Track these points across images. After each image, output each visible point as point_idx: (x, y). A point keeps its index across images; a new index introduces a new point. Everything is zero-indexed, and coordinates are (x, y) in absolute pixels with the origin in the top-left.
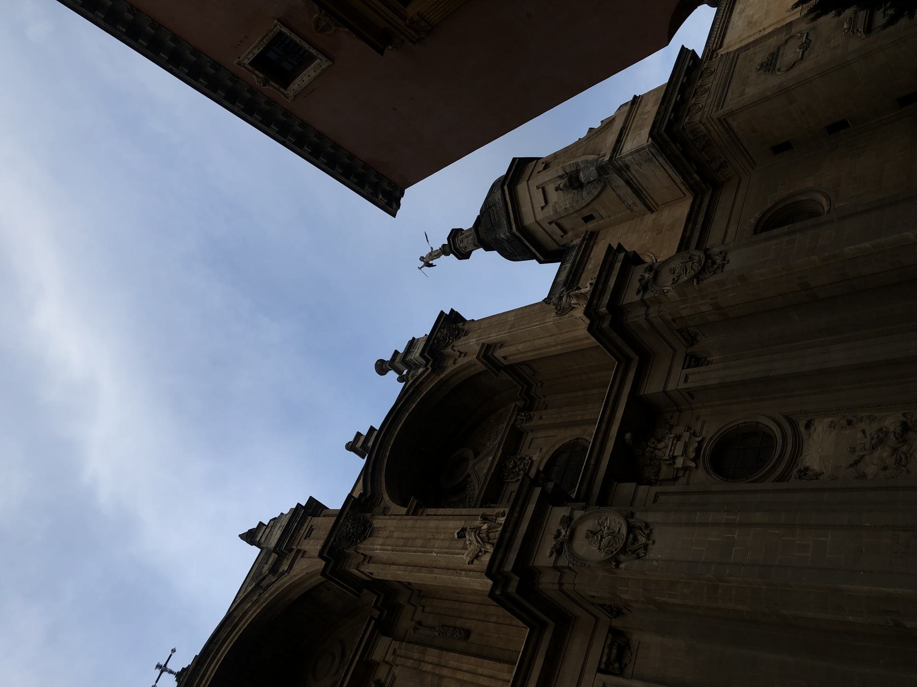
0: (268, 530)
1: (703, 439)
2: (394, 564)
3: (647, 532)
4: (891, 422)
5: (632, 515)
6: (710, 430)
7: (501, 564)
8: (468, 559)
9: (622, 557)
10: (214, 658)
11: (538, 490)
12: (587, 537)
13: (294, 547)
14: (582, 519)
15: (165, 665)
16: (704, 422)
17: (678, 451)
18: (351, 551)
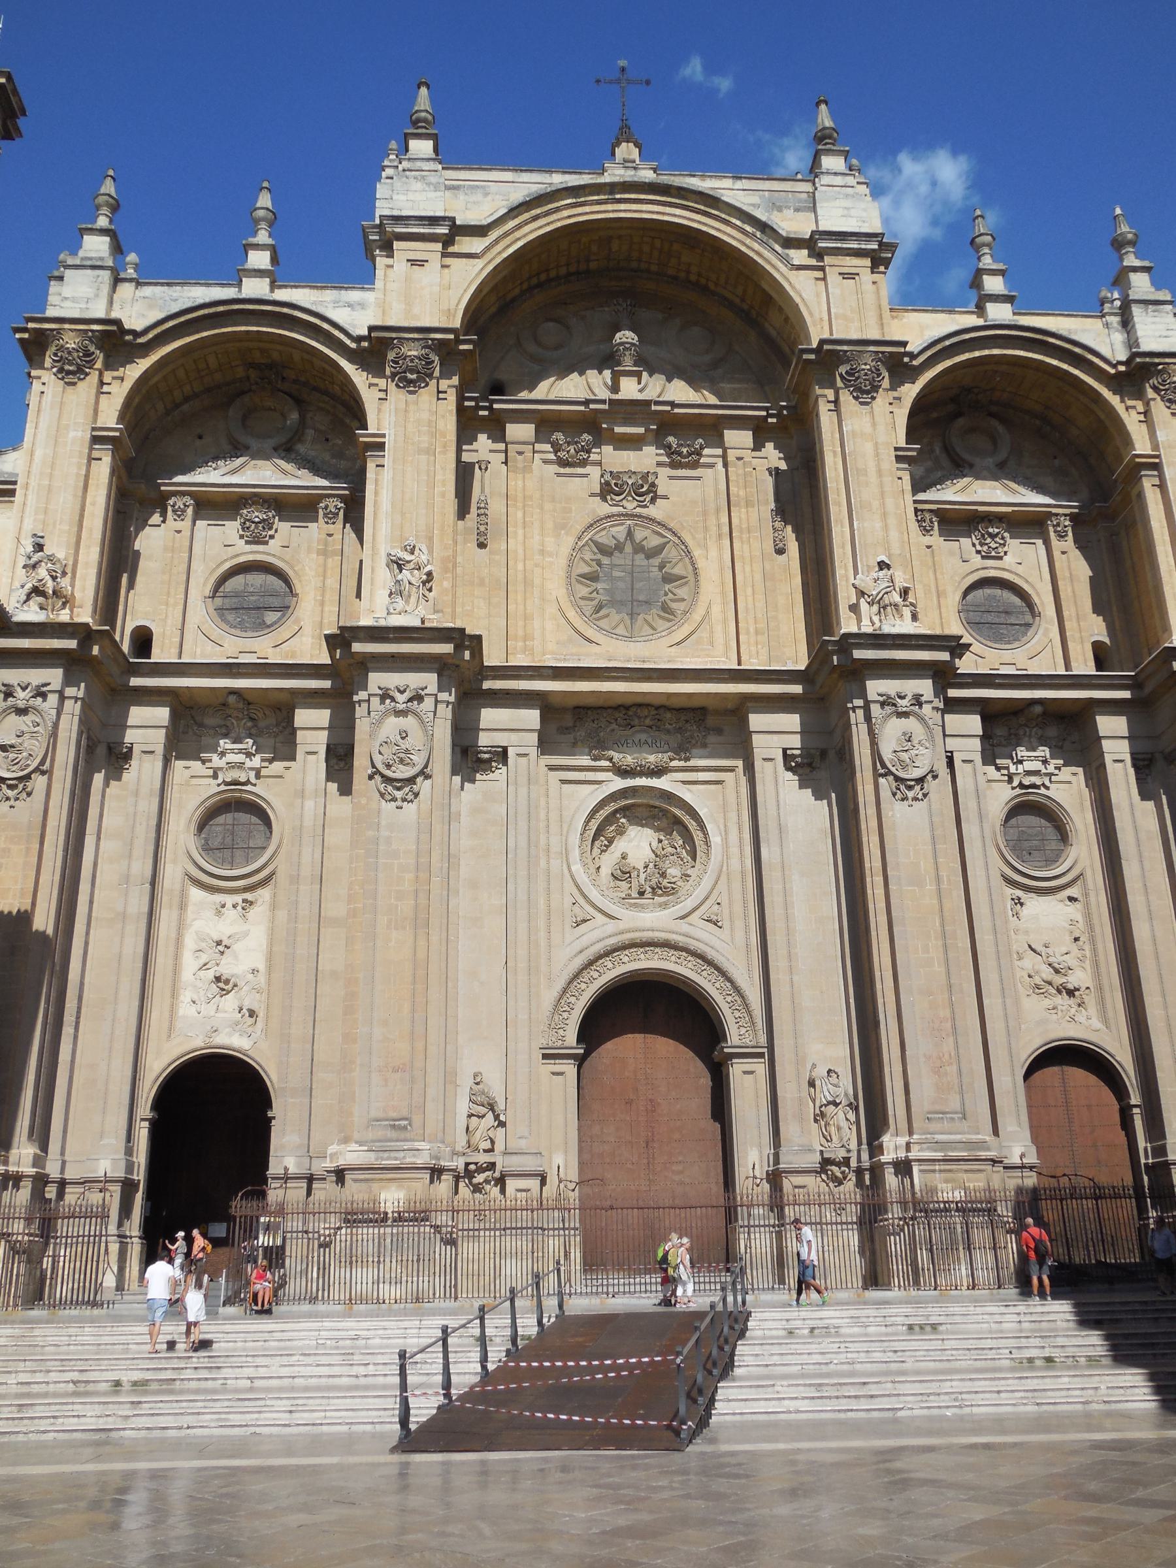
0: (839, 180)
1: (1047, 788)
3: (920, 796)
4: (1079, 978)
5: (935, 777)
6: (1058, 793)
7: (860, 646)
8: (857, 582)
9: (891, 778)
11: (945, 656)
12: (904, 734)
14: (921, 719)
15: (629, 82)
16: (1070, 782)
17: (1028, 766)
18: (839, 383)
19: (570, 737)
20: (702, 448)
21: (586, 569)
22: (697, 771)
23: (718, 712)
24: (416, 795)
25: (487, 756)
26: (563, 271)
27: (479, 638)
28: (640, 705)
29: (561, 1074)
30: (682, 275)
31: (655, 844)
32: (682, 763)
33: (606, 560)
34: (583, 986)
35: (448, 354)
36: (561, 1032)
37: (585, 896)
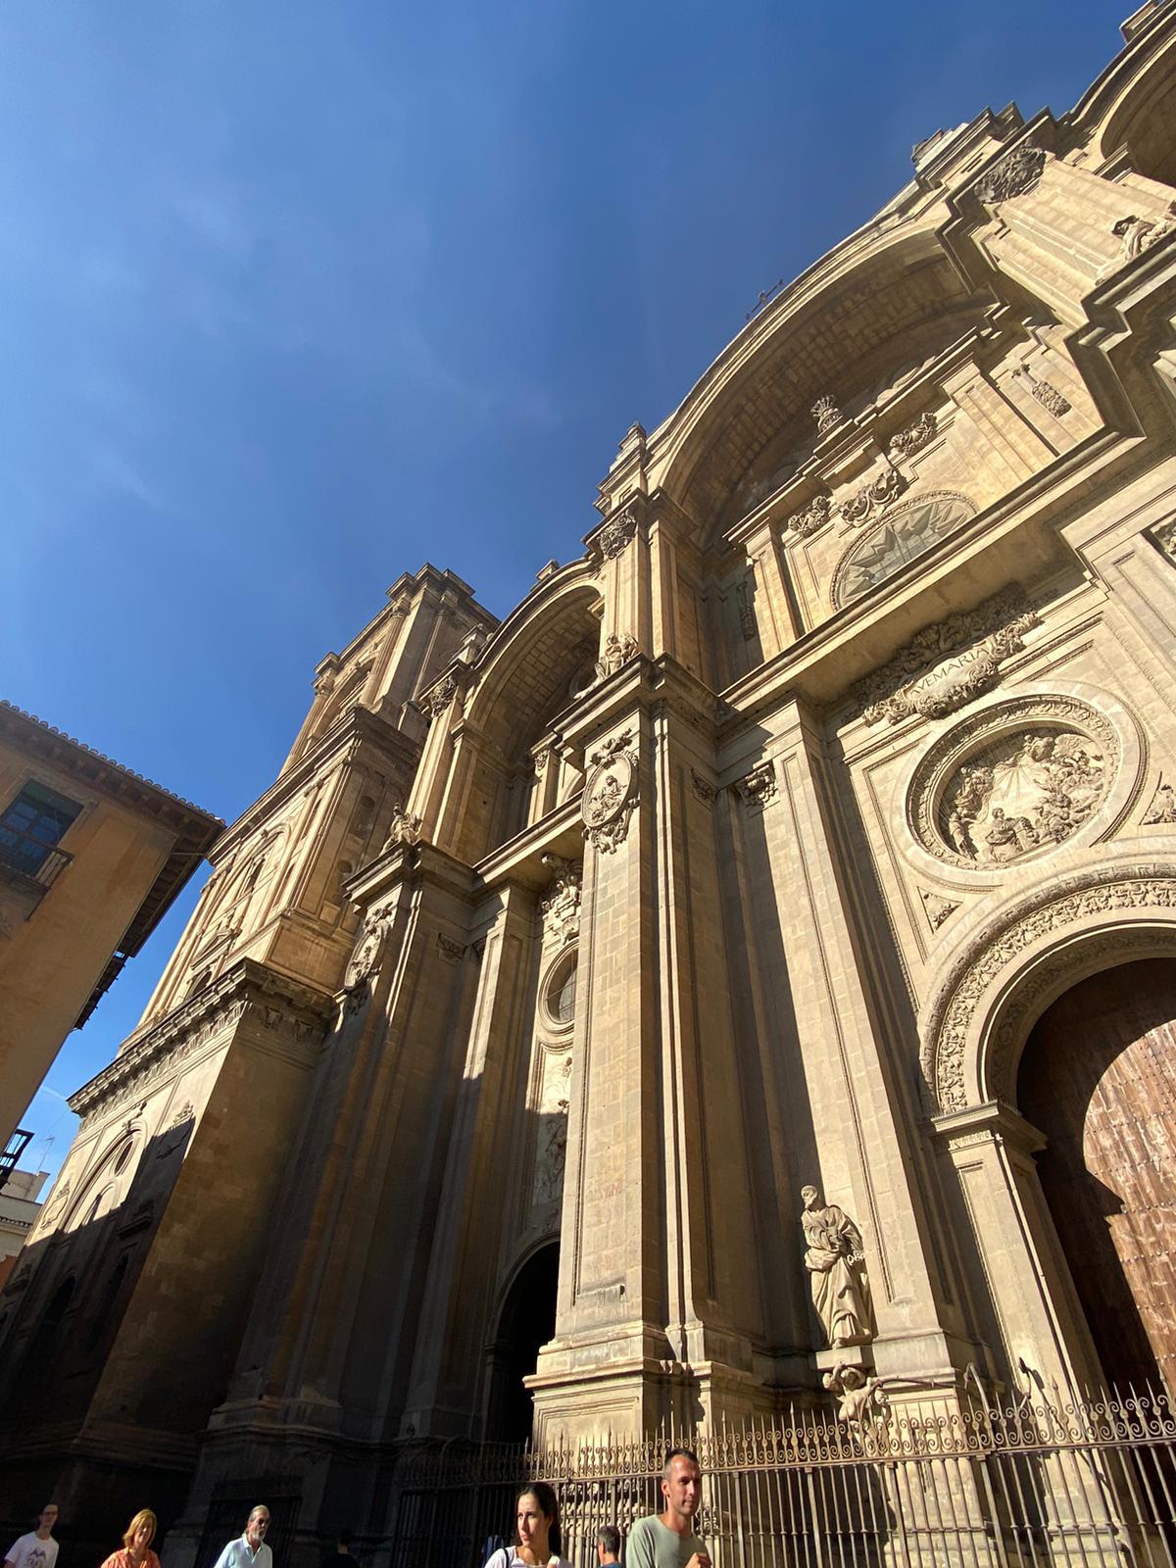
2: (1025, 252)
10: (793, 303)
13: (943, 181)
19: (861, 720)
20: (932, 422)
21: (850, 588)
22: (1042, 653)
23: (1035, 579)
24: (626, 832)
25: (754, 782)
26: (770, 431)
27: (664, 657)
28: (920, 632)
29: (976, 1166)
30: (866, 347)
31: (1043, 777)
32: (1018, 656)
33: (872, 570)
34: (970, 1002)
35: (647, 516)
36: (956, 1091)
37: (937, 880)
